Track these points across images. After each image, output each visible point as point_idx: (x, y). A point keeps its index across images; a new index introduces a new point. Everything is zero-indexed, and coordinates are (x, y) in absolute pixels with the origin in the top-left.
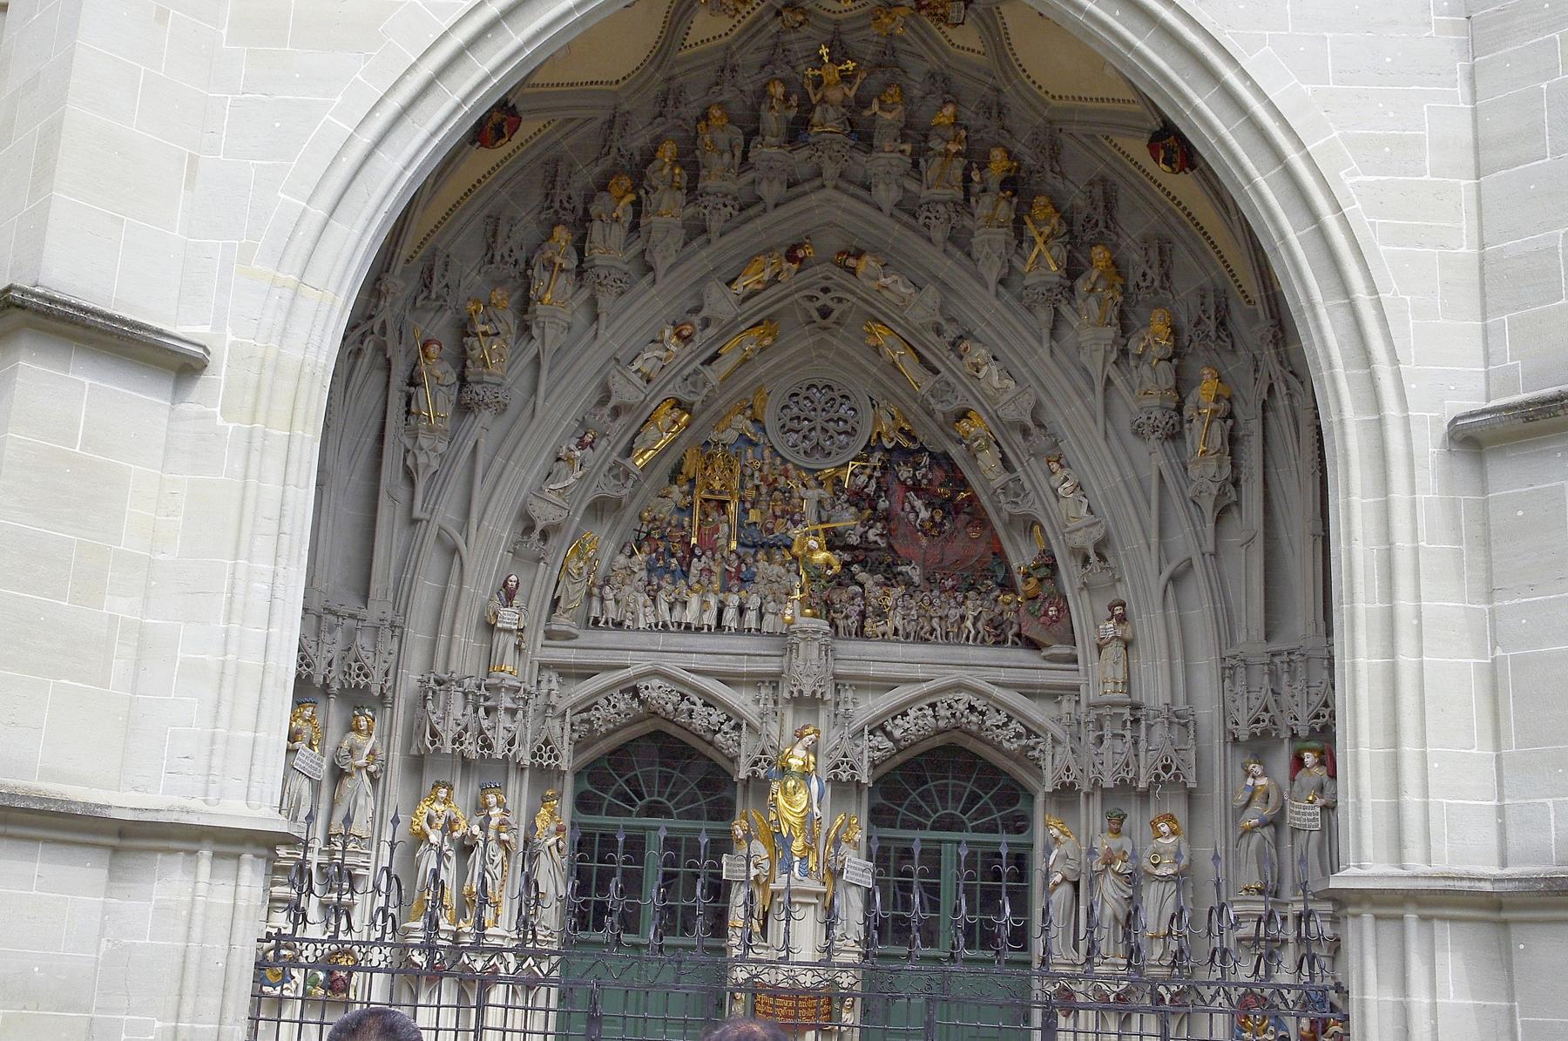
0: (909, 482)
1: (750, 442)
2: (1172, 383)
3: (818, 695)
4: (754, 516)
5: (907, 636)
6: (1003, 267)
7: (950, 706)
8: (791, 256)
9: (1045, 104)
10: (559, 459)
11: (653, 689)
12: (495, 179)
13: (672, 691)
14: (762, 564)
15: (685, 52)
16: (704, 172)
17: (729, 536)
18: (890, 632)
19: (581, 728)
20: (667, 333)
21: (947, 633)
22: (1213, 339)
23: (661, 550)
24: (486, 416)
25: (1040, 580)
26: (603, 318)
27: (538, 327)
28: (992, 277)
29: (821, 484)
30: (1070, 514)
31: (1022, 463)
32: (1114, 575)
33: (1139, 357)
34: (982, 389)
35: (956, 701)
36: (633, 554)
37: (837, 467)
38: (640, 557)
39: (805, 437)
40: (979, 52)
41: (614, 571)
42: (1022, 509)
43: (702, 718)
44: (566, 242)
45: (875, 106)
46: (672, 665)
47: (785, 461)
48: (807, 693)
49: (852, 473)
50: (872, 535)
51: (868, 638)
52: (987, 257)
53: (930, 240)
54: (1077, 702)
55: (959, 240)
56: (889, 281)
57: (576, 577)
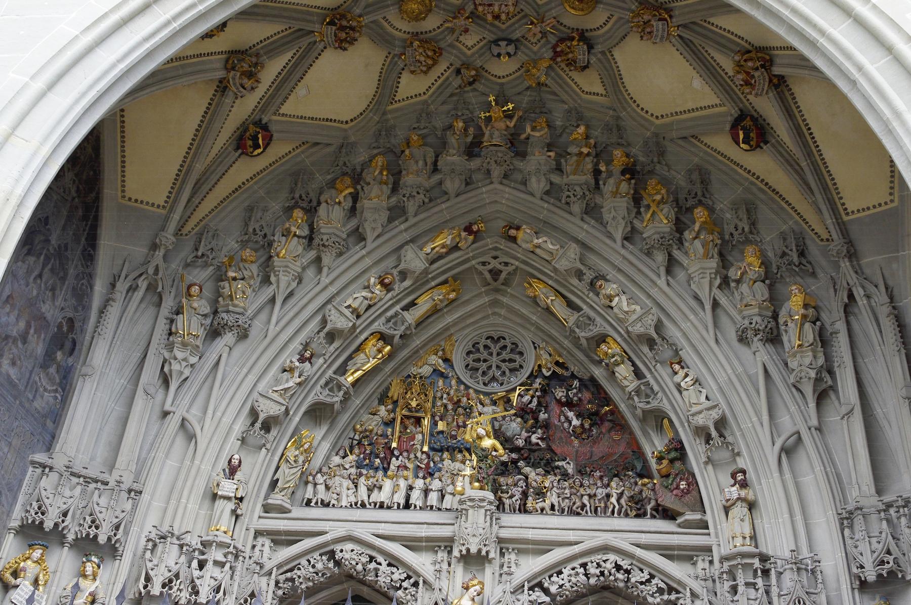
0: (564, 399)
1: (442, 375)
2: (767, 295)
3: (484, 553)
4: (441, 426)
7: (599, 565)
8: (468, 229)
9: (652, 123)
10: (285, 371)
11: (347, 552)
12: (256, 183)
13: (363, 553)
14: (447, 462)
15: (396, 106)
16: (404, 172)
17: (423, 442)
18: (548, 509)
19: (285, 586)
20: (372, 280)
22: (797, 264)
23: (368, 452)
24: (229, 338)
26: (325, 270)
27: (275, 276)
28: (618, 236)
29: (494, 403)
30: (692, 402)
31: (650, 370)
32: (733, 450)
33: (738, 282)
34: (616, 314)
35: (605, 561)
37: (507, 391)
38: (351, 458)
39: (484, 373)
40: (602, 95)
41: (330, 468)
42: (654, 404)
43: (386, 576)
44: (302, 221)
45: (528, 130)
46: (364, 532)
47: (467, 387)
48: (474, 550)
49: (519, 395)
50: (534, 439)
51: (530, 513)
52: (614, 218)
53: (571, 214)
54: (711, 562)
55: (592, 211)
56: (540, 241)
57: (293, 463)
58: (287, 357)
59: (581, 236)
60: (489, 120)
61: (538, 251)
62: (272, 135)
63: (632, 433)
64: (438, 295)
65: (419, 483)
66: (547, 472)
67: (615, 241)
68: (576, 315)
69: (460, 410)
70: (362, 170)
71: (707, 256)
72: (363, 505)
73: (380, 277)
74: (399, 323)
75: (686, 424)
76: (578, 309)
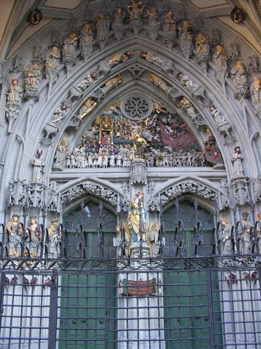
0: (166, 122)
1: (116, 114)
2: (246, 81)
3: (143, 182)
4: (118, 134)
5: (170, 165)
6: (190, 53)
7: (186, 185)
8: (126, 54)
10: (55, 114)
18: (164, 165)
21: (182, 164)
24: (31, 101)
25: (211, 145)
26: (68, 72)
28: (187, 57)
29: (138, 124)
33: (234, 75)
34: (187, 88)
36: (81, 147)
42: (203, 123)
43: (104, 193)
47: (127, 118)
48: (139, 181)
50: (155, 138)
51: (157, 166)
54: (227, 181)
55: (176, 46)
56: (156, 58)
58: (56, 108)
59: (172, 57)
60: (131, 9)
61: (155, 63)
62: (42, 15)
63: (193, 135)
64: (115, 81)
65: (113, 157)
66: (162, 151)
67: (186, 59)
68: (171, 89)
69: (125, 128)
70: (80, 30)
71: (222, 65)
72: (91, 166)
73: (91, 74)
74: (100, 93)
75: (216, 131)
76: (172, 86)
